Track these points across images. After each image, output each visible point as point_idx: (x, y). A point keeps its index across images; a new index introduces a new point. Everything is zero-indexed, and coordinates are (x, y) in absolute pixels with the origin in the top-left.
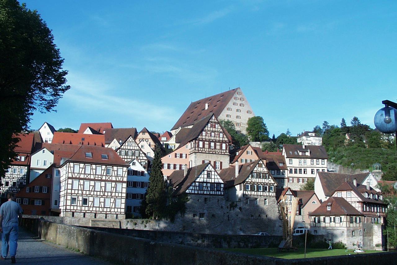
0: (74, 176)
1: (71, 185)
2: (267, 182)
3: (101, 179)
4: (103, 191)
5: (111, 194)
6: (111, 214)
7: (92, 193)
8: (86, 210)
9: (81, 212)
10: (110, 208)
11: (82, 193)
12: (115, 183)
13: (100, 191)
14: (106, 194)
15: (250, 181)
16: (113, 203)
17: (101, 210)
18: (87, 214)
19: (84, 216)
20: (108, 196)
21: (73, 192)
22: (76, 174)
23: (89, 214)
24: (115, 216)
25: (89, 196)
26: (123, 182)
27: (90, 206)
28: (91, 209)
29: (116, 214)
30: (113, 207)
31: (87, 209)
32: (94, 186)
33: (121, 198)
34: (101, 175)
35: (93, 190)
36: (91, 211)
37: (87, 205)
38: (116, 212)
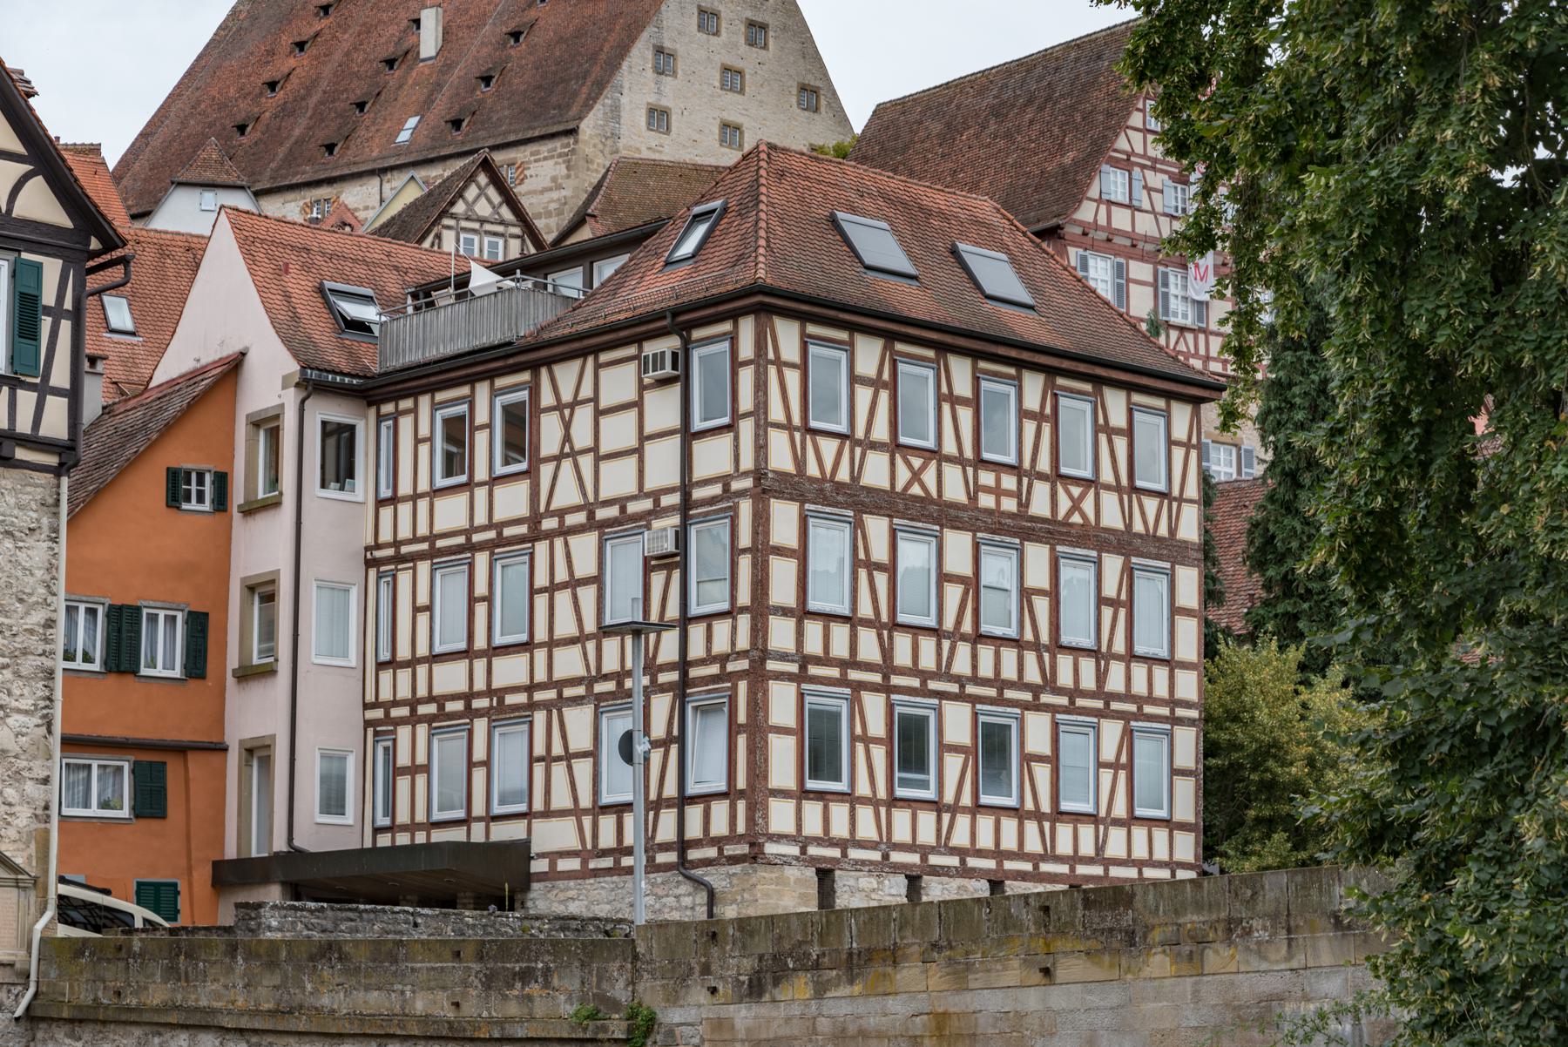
9: (885, 867)
11: (887, 652)
25: (941, 695)
35: (967, 627)
37: (930, 794)
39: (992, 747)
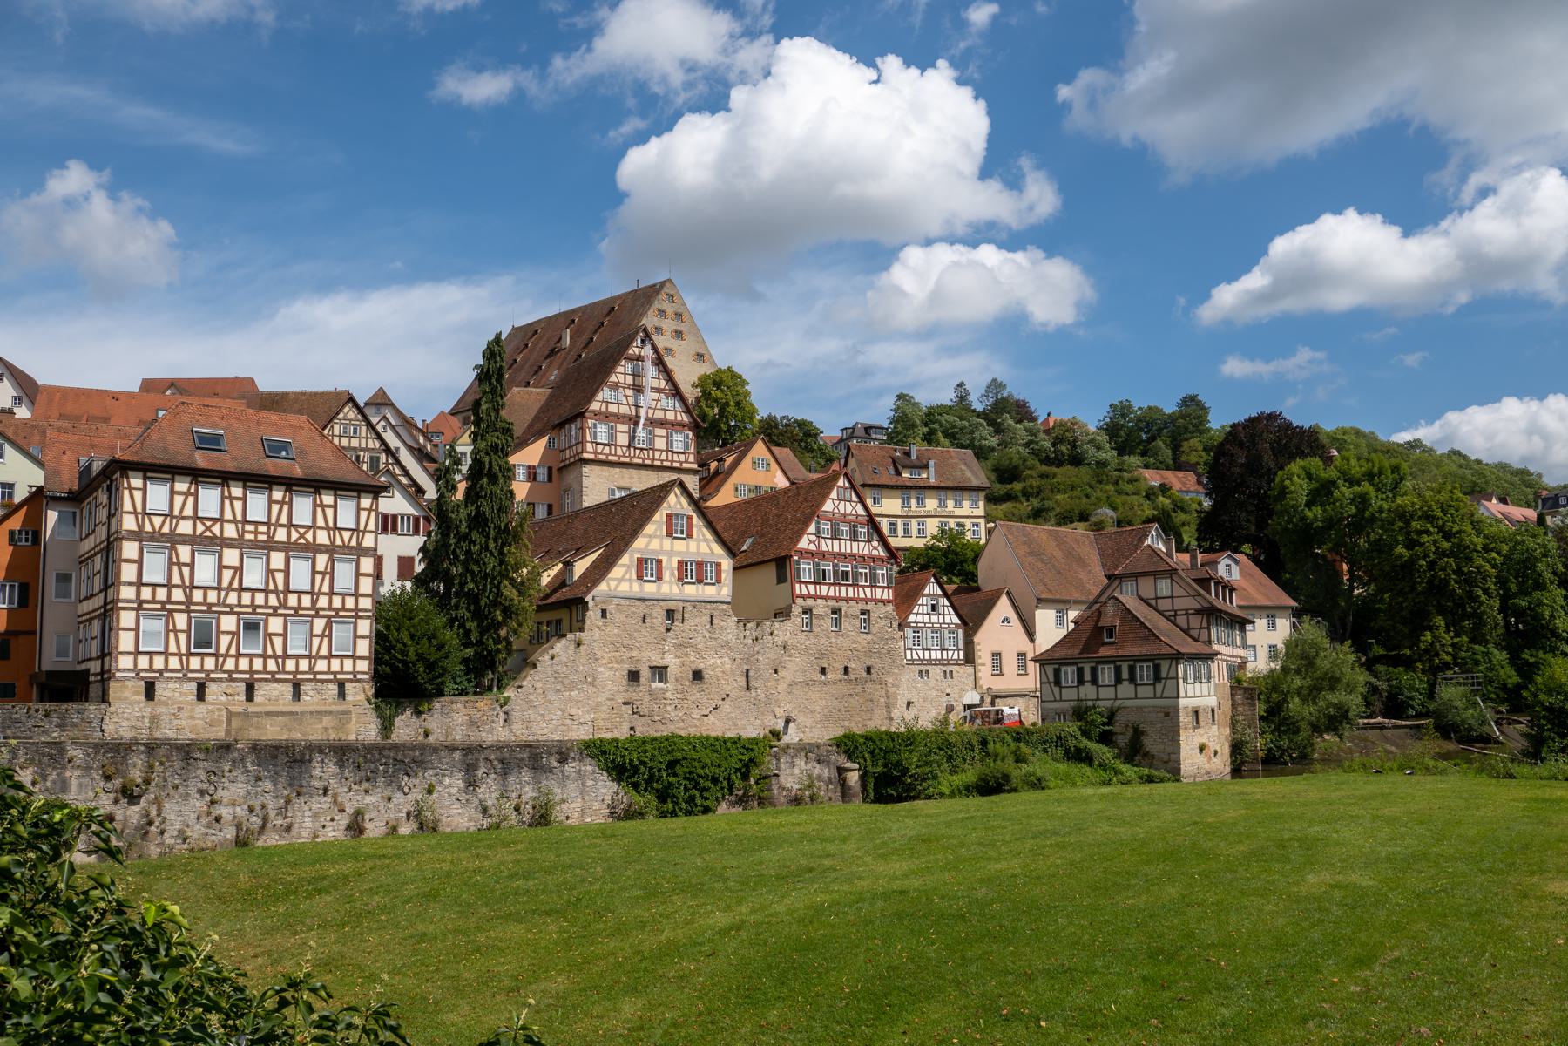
0: (148, 528)
1: (134, 566)
3: (271, 538)
4: (281, 587)
5: (314, 602)
6: (315, 680)
7: (232, 598)
8: (206, 667)
10: (309, 657)
11: (189, 597)
12: (326, 557)
13: (266, 591)
14: (292, 600)
16: (322, 636)
17: (271, 665)
18: (212, 688)
19: (201, 694)
20: (299, 607)
21: (146, 593)
22: (157, 521)
23: (224, 684)
24: (334, 688)
26: (360, 551)
27: (223, 650)
28: (230, 664)
29: (335, 680)
30: (324, 652)
31: (210, 663)
32: (239, 570)
33: (357, 617)
34: (268, 524)
35: (235, 585)
36: (230, 672)
37: (212, 651)
38: (335, 673)
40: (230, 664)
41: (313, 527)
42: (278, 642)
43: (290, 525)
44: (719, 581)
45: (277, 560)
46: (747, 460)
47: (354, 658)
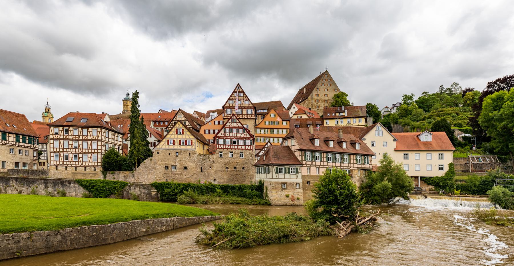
2: (242, 136)
7: (72, 150)
14: (84, 151)
15: (222, 135)
26: (98, 140)
31: (68, 163)
32: (72, 145)
39: (76, 156)
40: (72, 163)
41: (87, 136)
42: (81, 159)
43: (83, 136)
44: (192, 145)
45: (80, 142)
46: (269, 115)
47: (97, 162)
